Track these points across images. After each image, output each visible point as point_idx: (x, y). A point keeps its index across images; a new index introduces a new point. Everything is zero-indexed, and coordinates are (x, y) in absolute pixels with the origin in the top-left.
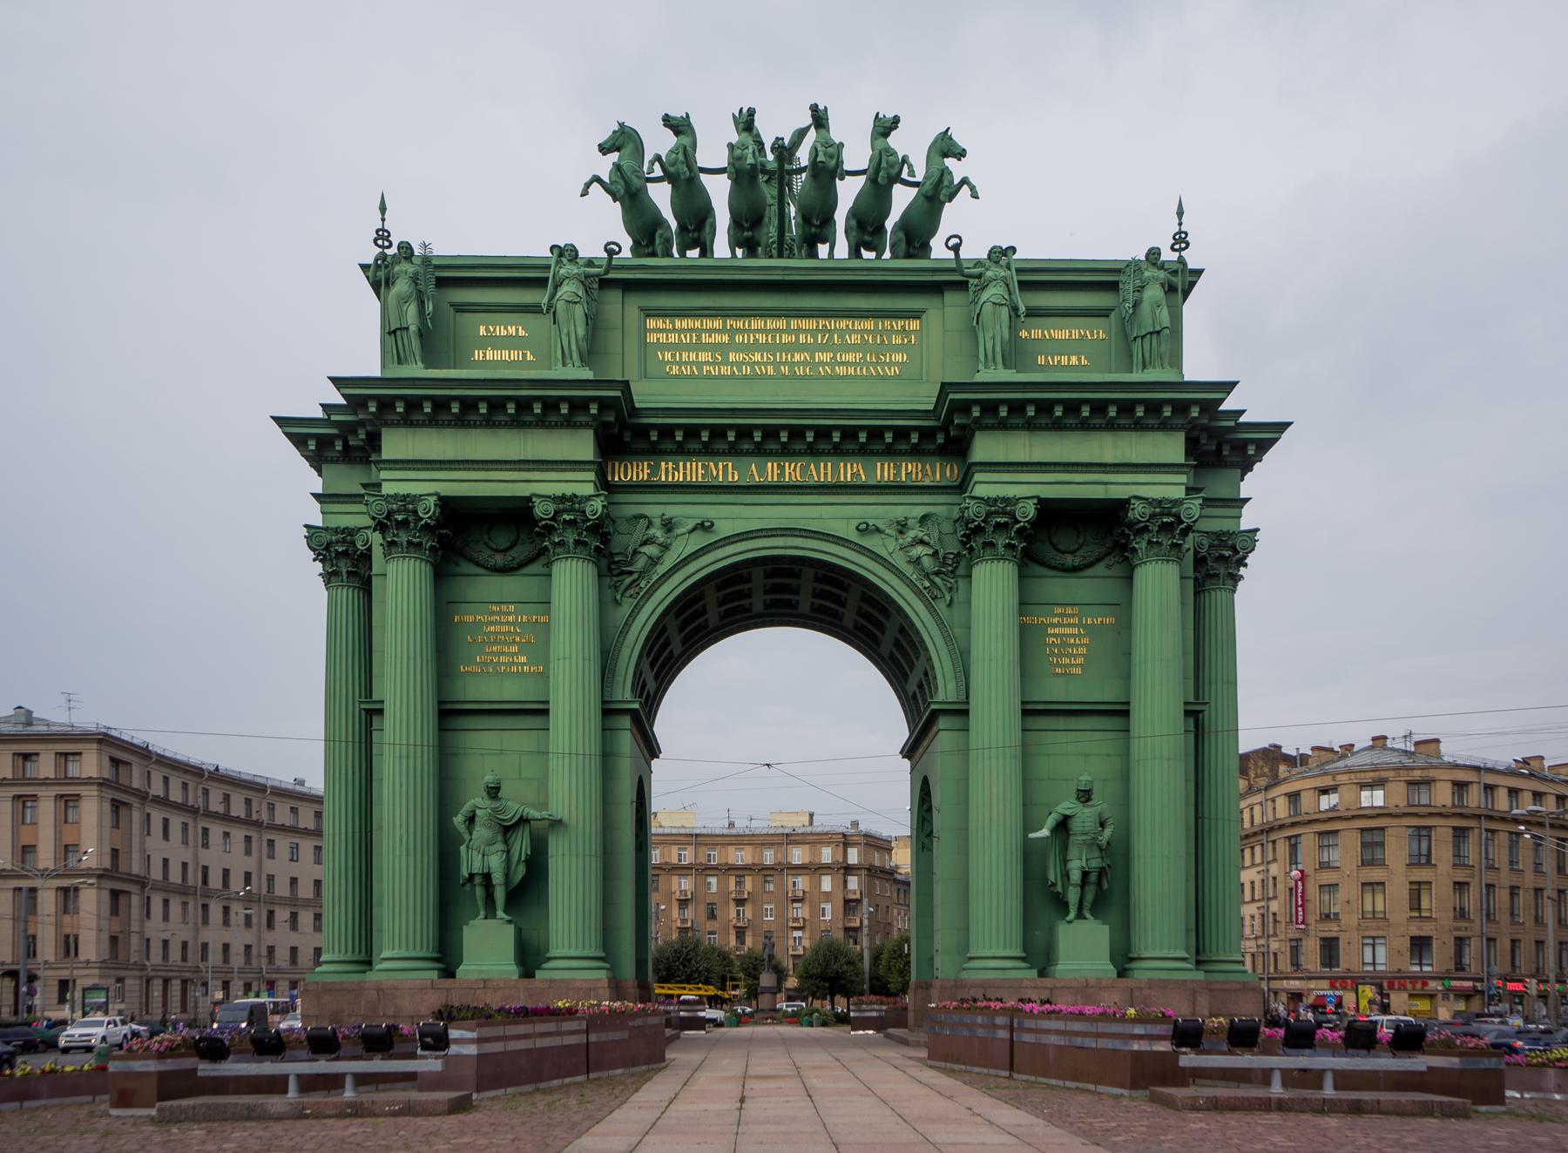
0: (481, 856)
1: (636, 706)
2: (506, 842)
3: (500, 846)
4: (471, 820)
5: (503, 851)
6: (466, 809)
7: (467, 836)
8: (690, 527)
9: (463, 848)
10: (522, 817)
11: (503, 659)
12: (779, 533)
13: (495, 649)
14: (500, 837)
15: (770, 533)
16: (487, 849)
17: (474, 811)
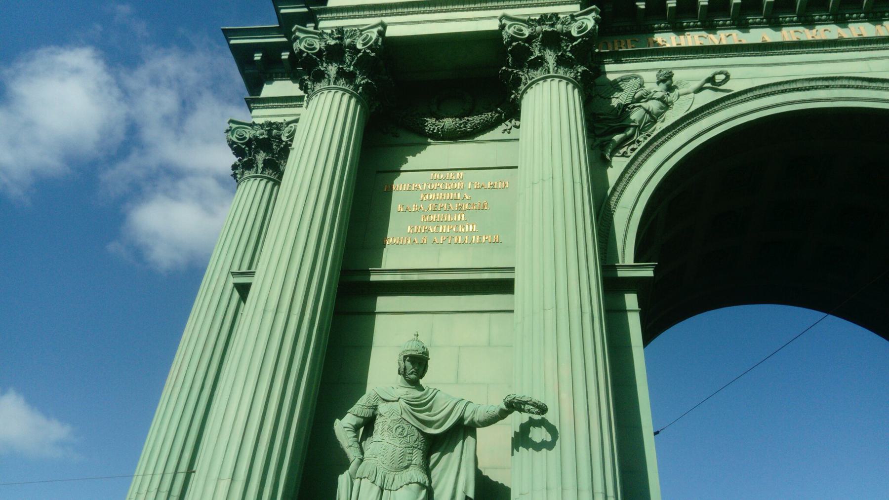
0: (376, 489)
1: (649, 273)
2: (427, 470)
3: (416, 474)
4: (367, 426)
5: (422, 486)
6: (360, 407)
7: (352, 454)
8: (696, 85)
9: (343, 480)
10: (461, 419)
11: (444, 228)
12: (820, 83)
13: (433, 218)
14: (417, 457)
15: (807, 84)
16: (390, 477)
17: (375, 408)
